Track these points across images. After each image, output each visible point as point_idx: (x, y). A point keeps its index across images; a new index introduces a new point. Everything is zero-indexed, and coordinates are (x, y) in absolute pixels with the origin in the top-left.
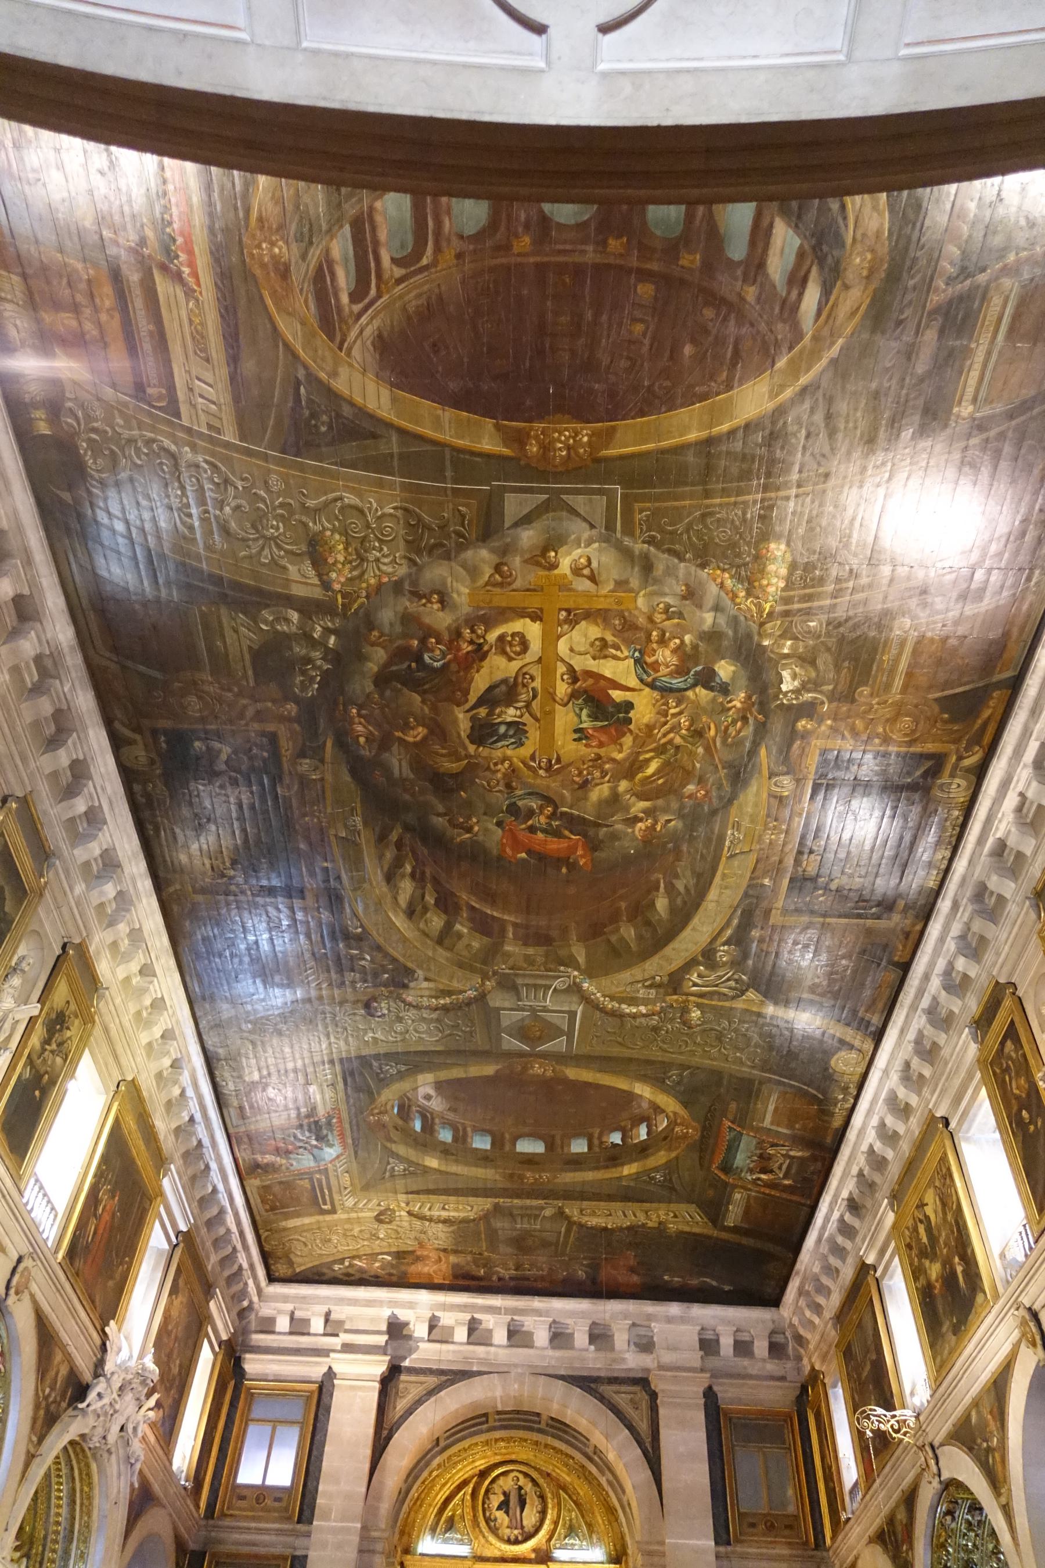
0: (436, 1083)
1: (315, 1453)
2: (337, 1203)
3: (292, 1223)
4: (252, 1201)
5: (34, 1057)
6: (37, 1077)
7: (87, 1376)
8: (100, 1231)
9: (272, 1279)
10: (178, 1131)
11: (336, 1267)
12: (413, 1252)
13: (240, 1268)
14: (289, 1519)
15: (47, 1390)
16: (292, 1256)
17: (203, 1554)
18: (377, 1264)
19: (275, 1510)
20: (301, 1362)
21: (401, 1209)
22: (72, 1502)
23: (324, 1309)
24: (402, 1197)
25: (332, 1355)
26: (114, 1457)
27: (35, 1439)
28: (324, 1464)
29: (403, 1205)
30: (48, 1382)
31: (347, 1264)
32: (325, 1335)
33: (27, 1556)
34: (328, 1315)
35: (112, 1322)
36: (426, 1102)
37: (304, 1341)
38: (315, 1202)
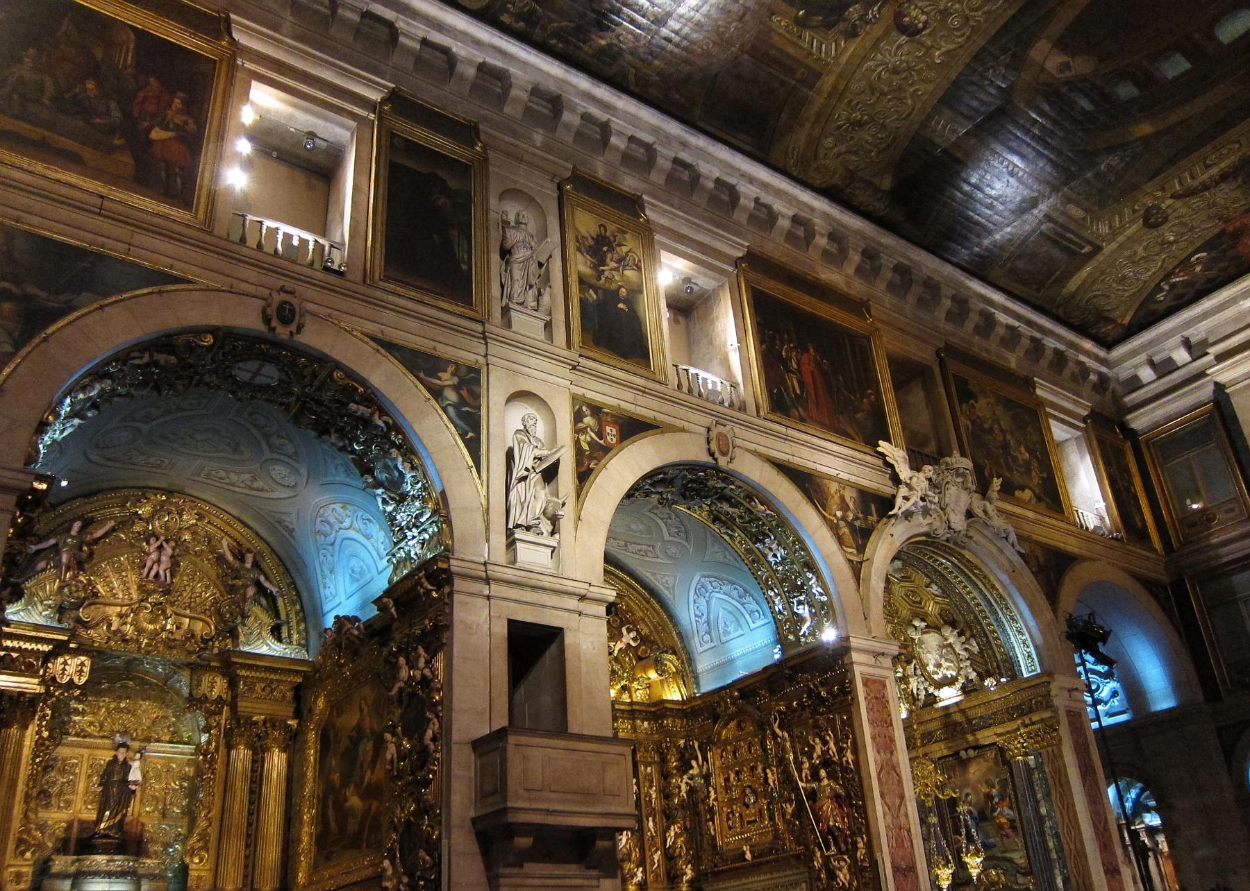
0: (1055, 45)
2: (1090, 238)
3: (1074, 284)
4: (1016, 292)
5: (594, 281)
6: (613, 296)
7: (887, 489)
8: (808, 379)
9: (1109, 345)
10: (859, 270)
11: (1160, 297)
12: (1223, 232)
13: (1057, 352)
15: (839, 514)
16: (1106, 314)
17: (1184, 580)
18: (1198, 269)
19: (1232, 519)
20: (1183, 395)
21: (1163, 199)
22: (975, 585)
23: (1178, 339)
24: (1148, 187)
25: (1208, 372)
26: (976, 537)
29: (1159, 194)
31: (1166, 287)
32: (1194, 360)
33: (973, 636)
34: (1187, 344)
35: (881, 442)
36: (1068, 74)
37: (1176, 376)
38: (1072, 253)
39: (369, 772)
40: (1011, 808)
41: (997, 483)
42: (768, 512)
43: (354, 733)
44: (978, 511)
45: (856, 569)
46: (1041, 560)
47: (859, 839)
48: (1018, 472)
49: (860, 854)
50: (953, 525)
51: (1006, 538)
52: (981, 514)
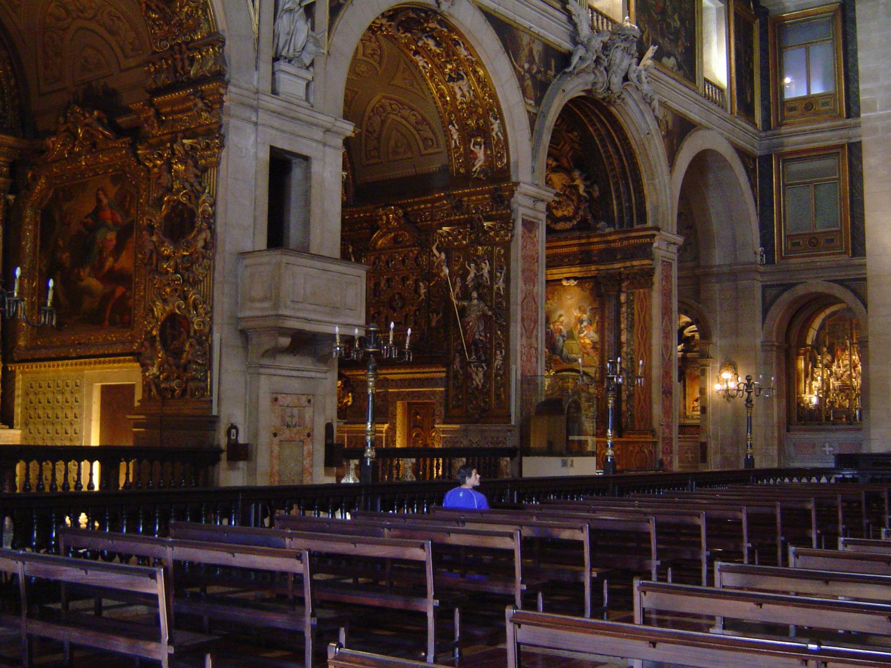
1: (851, 60)
14: (840, 116)
15: (526, 66)
19: (826, 112)
27: (532, 102)
28: (861, 67)
30: (524, 59)
39: (111, 259)
40: (596, 332)
41: (651, 51)
42: (470, 57)
43: (90, 220)
44: (633, 76)
45: (533, 119)
46: (670, 124)
47: (498, 352)
48: (669, 39)
49: (498, 362)
50: (613, 87)
51: (650, 104)
52: (635, 80)
